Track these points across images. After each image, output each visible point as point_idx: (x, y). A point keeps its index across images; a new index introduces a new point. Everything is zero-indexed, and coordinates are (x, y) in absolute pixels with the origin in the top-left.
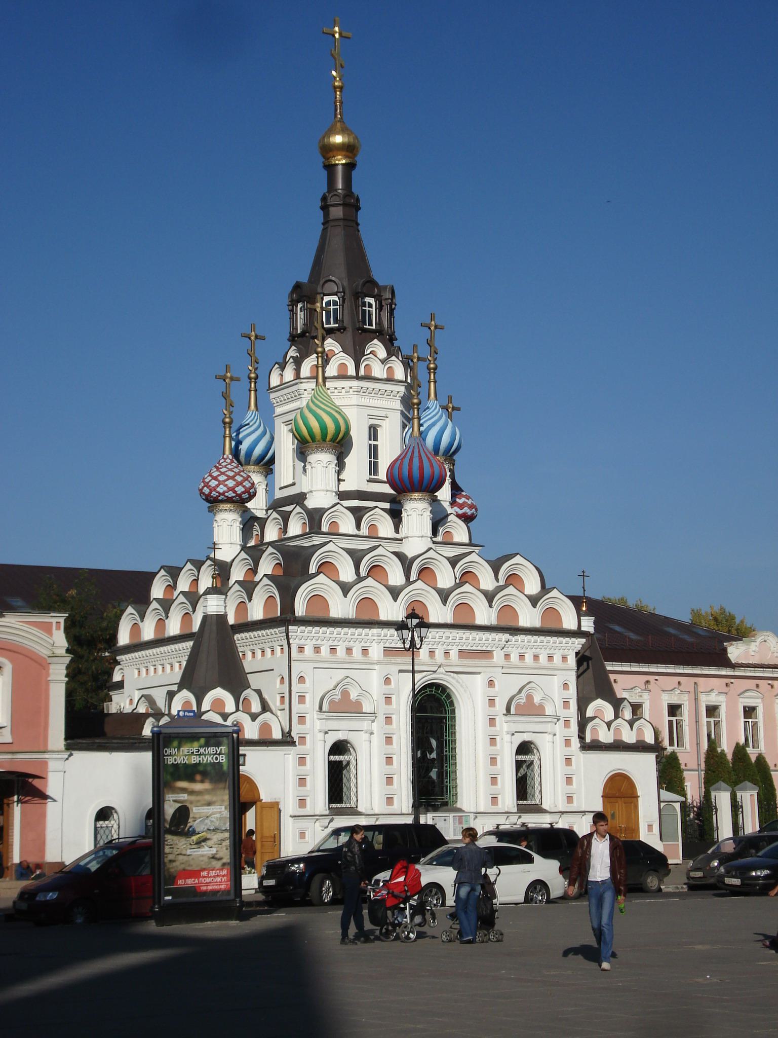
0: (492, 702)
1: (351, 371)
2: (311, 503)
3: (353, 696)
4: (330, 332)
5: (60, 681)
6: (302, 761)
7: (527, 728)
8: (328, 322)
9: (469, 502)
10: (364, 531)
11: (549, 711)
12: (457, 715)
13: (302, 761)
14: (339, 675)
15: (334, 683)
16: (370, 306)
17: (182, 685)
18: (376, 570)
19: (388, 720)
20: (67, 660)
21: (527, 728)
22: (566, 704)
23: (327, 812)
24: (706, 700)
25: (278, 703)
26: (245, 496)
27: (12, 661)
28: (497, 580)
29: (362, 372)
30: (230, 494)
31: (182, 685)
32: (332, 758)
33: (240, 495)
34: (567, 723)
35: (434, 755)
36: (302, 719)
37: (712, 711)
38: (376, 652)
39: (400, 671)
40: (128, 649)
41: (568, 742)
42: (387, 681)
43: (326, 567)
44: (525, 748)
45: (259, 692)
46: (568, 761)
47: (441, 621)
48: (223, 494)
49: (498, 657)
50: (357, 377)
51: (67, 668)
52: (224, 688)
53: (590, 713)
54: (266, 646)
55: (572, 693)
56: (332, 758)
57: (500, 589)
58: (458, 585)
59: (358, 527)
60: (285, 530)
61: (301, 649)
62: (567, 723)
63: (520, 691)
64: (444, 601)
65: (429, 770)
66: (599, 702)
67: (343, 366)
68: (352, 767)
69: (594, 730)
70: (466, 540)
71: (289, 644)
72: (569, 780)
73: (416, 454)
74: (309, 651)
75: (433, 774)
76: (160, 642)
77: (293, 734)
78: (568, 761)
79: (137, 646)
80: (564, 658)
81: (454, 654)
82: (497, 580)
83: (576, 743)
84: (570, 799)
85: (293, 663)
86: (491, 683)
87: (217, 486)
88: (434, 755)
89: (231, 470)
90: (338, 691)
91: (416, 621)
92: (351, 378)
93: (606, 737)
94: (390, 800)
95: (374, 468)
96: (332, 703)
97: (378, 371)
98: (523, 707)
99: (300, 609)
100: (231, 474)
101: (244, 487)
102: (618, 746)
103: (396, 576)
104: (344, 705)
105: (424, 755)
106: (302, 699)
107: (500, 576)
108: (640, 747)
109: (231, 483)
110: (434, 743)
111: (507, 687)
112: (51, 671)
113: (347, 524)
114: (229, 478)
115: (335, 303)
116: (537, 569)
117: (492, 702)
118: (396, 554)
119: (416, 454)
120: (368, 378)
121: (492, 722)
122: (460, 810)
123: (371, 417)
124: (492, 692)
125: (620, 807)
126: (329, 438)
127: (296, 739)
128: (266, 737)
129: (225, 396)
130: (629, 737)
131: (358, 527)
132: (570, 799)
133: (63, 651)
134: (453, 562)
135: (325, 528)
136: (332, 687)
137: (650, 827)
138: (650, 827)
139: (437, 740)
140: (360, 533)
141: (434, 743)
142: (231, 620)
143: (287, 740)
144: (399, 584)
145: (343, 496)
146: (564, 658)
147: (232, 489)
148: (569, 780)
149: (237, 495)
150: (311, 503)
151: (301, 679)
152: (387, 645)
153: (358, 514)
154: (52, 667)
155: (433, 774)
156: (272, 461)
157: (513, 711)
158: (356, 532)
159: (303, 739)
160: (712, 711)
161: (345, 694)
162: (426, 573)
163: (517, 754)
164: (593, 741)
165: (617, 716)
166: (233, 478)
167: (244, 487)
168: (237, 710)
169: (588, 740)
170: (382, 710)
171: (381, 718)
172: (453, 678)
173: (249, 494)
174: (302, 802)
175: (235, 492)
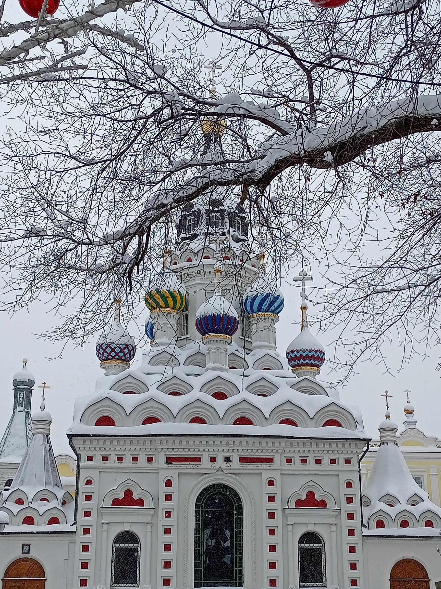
14: (123, 478)
19: (168, 514)
32: (117, 545)
35: (228, 544)
46: (352, 549)
65: (223, 555)
81: (235, 459)
86: (271, 483)
105: (218, 544)
110: (228, 533)
124: (271, 490)
139: (232, 531)
141: (228, 533)
155: (227, 559)
171: (162, 514)
172: (233, 479)
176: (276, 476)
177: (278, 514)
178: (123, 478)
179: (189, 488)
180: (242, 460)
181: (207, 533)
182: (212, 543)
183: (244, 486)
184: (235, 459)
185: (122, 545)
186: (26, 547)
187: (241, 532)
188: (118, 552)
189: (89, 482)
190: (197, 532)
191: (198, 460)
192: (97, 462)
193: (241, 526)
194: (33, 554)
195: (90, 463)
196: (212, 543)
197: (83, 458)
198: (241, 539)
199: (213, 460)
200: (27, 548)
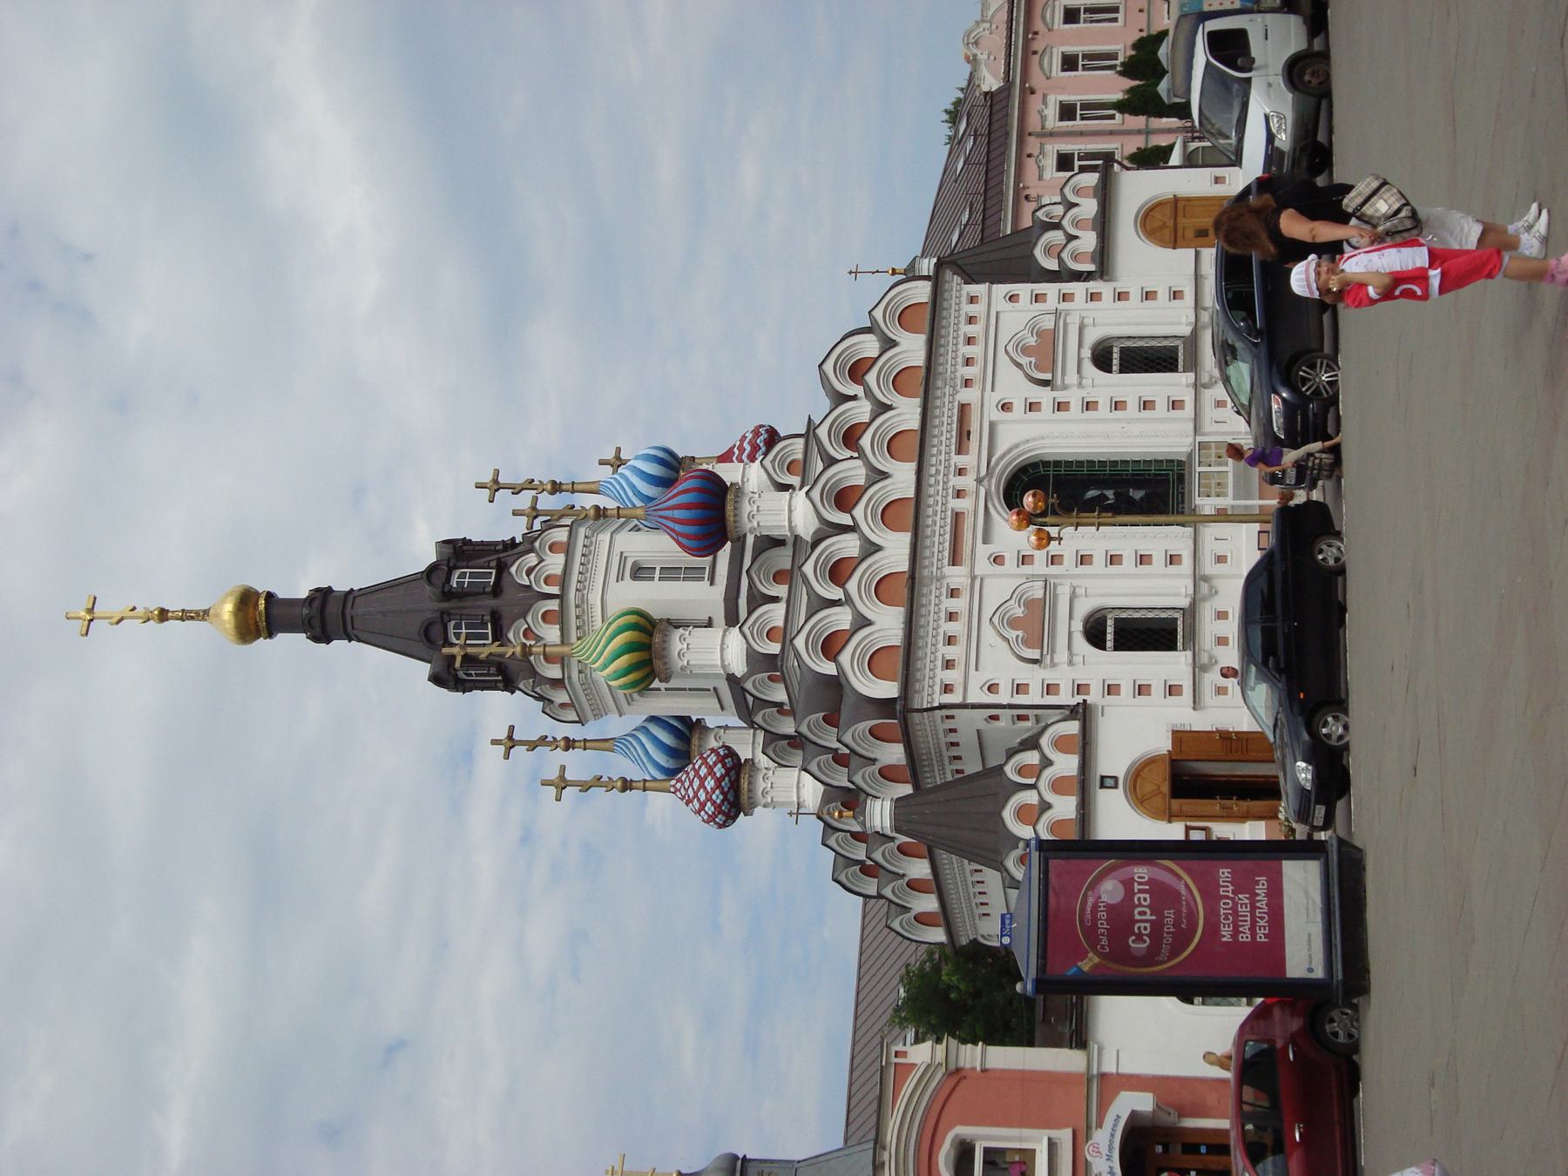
0: (1032, 407)
1: (553, 605)
2: (739, 667)
3: (1019, 612)
5: (983, 1053)
6: (1112, 689)
7: (1075, 353)
8: (485, 637)
9: (749, 436)
10: (781, 590)
11: (1048, 323)
12: (1051, 459)
13: (1112, 689)
14: (989, 634)
15: (1000, 640)
16: (463, 575)
17: (1000, 867)
18: (838, 572)
20: (953, 1042)
21: (1075, 353)
22: (1038, 298)
23: (1189, 654)
24: (1052, 121)
25: (1028, 724)
27: (951, 1127)
28: (854, 398)
29: (555, 590)
31: (1000, 867)
32: (1110, 644)
33: (728, 771)
34: (1066, 297)
35: (1110, 494)
36: (1050, 689)
37: (1067, 112)
38: (957, 576)
39: (986, 541)
40: (950, 933)
41: (1094, 297)
42: (998, 560)
43: (831, 646)
44: (1102, 359)
45: (1011, 753)
46: (1121, 296)
47: (913, 478)
49: (968, 395)
50: (560, 597)
51: (964, 1041)
52: (1003, 807)
53: (1052, 265)
54: (943, 740)
55: (1024, 290)
56: (1110, 644)
57: (869, 393)
58: (862, 455)
59: (775, 599)
60: (779, 705)
61: (947, 689)
62: (1066, 297)
63: (1019, 365)
64: (884, 475)
65: (1131, 500)
66: (1038, 252)
67: (546, 617)
68: (1124, 615)
69: (1075, 257)
70: (802, 441)
71: (942, 707)
72: (1149, 295)
73: (668, 513)
74: (952, 676)
75: (1137, 495)
76: (937, 885)
77: (1073, 702)
78: (1121, 296)
79: (945, 917)
80: (973, 300)
81: (960, 461)
82: (854, 398)
83: (1093, 286)
84: (1176, 295)
85: (970, 701)
87: (714, 803)
88: (1110, 494)
89: (691, 783)
90: (1012, 634)
91: (910, 515)
92: (561, 605)
93: (1088, 241)
94: (1173, 559)
95: (692, 574)
96: (1027, 643)
97: (555, 563)
98: (1043, 359)
99: (888, 689)
100: (696, 783)
101: (715, 764)
102: (1104, 224)
103: (848, 546)
104: (1033, 626)
106: (1020, 689)
107: (851, 393)
108: (1105, 194)
110: (1092, 493)
111: (1013, 384)
112: (968, 1066)
113: (775, 614)
114: (702, 786)
115: (458, 626)
116: (843, 339)
117: (1032, 407)
118: (815, 545)
119: (668, 513)
120: (563, 580)
122: (1190, 455)
123: (620, 577)
124: (1019, 406)
125: (1189, 223)
127: (1079, 699)
128: (1079, 741)
130: (1089, 207)
131: (775, 599)
132: (1176, 295)
133: (940, 1048)
134: (831, 461)
135: (775, 648)
136: (1005, 644)
137: (1218, 180)
138: (1218, 180)
141: (1092, 493)
142: (907, 789)
143: (1082, 712)
144: (858, 543)
145: (732, 619)
146: (973, 300)
147: (719, 781)
148: (1149, 295)
149: (727, 774)
150: (739, 667)
151: (992, 688)
152: (946, 561)
153: (758, 600)
154: (961, 1064)
155: (1137, 495)
156: (684, 720)
157: (1048, 376)
159: (1080, 689)
160: (1067, 112)
161: (1014, 623)
162: (844, 498)
163: (1110, 371)
164: (1093, 261)
165: (1057, 226)
166: (702, 780)
167: (715, 764)
168: (1033, 787)
169: (1092, 268)
172: (997, 464)
173: (726, 756)
174: (1173, 690)
175: (723, 777)
176: (992, 399)
177: (1061, 396)
178: (989, 634)
179: (1011, 536)
183: (1010, 450)
184: (960, 461)
185: (1110, 637)
186: (1107, 782)
189: (992, 688)
192: (952, 676)
195: (959, 690)
199: (959, 494)
200: (1109, 782)
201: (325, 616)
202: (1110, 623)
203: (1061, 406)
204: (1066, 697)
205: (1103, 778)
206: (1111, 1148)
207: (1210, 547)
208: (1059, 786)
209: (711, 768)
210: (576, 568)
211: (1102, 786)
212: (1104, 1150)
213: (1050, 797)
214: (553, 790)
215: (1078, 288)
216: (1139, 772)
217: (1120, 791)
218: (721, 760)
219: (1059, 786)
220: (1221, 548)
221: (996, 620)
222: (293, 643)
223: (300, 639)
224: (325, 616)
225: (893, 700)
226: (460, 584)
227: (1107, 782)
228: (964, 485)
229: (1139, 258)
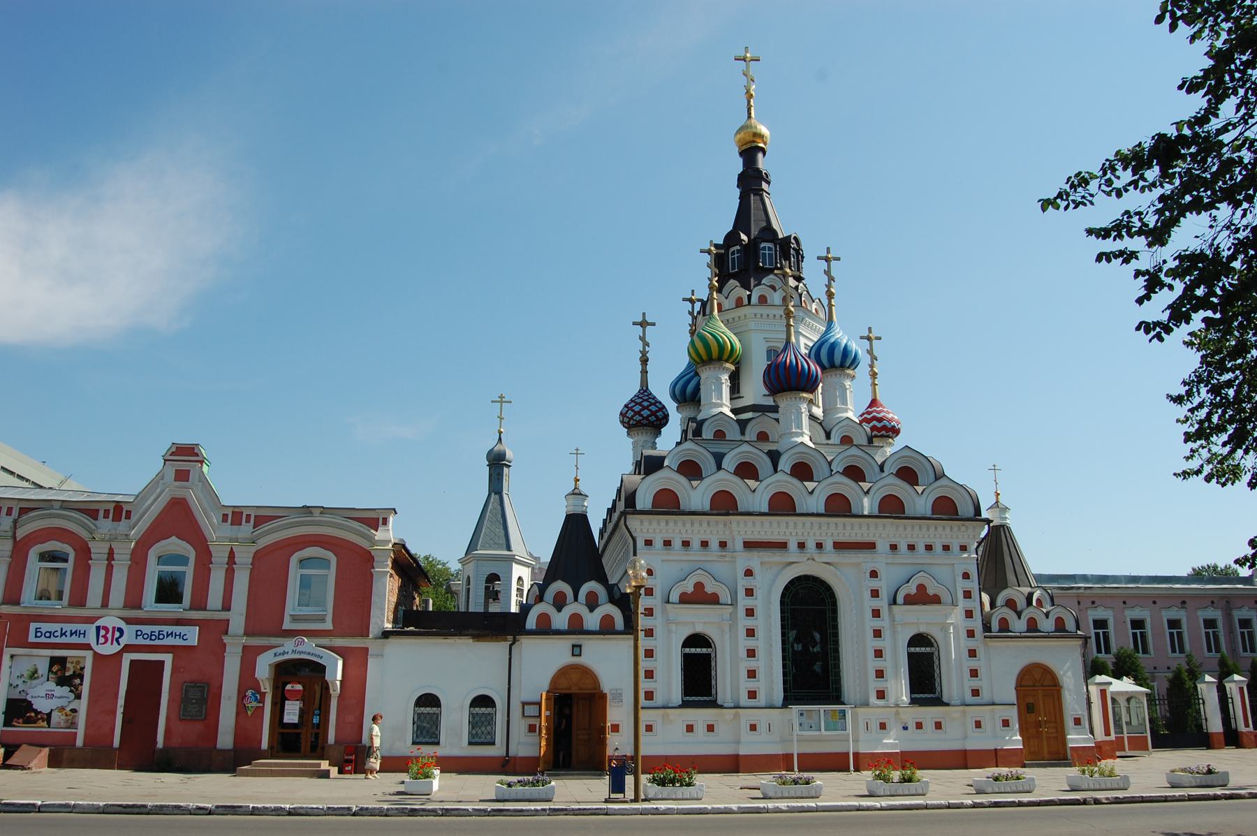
1: (746, 301)
4: (734, 276)
16: (770, 249)
26: (653, 418)
28: (882, 471)
30: (637, 418)
32: (687, 650)
33: (647, 418)
48: (632, 418)
56: (687, 650)
59: (743, 433)
71: (634, 539)
75: (817, 667)
105: (805, 647)
109: (637, 408)
110: (817, 636)
113: (733, 433)
117: (875, 593)
121: (876, 613)
124: (874, 583)
126: (725, 357)
129: (643, 338)
131: (743, 433)
137: (1077, 721)
140: (747, 438)
141: (817, 636)
147: (638, 413)
155: (817, 667)
157: (900, 599)
158: (739, 437)
166: (640, 404)
170: (744, 602)
177: (885, 613)
180: (839, 546)
181: (792, 634)
182: (798, 647)
185: (693, 650)
186: (577, 650)
187: (836, 635)
188: (688, 661)
190: (783, 635)
191: (783, 546)
193: (835, 627)
194: (585, 660)
196: (798, 647)
197: (640, 543)
198: (836, 642)
200: (577, 651)
201: (752, 182)
202: (704, 650)
203: (876, 613)
204: (643, 622)
205: (580, 646)
206: (301, 653)
207: (762, 717)
208: (576, 620)
209: (647, 408)
210: (772, 311)
211: (574, 646)
212: (300, 648)
213: (568, 611)
214: (640, 319)
215: (976, 624)
216: (586, 672)
217: (567, 659)
218: (653, 413)
219: (576, 620)
220: (762, 727)
221: (699, 572)
222: (738, 166)
223: (741, 170)
224: (752, 182)
225: (634, 506)
226: (764, 248)
227: (577, 650)
228: (810, 547)
229: (1002, 667)
